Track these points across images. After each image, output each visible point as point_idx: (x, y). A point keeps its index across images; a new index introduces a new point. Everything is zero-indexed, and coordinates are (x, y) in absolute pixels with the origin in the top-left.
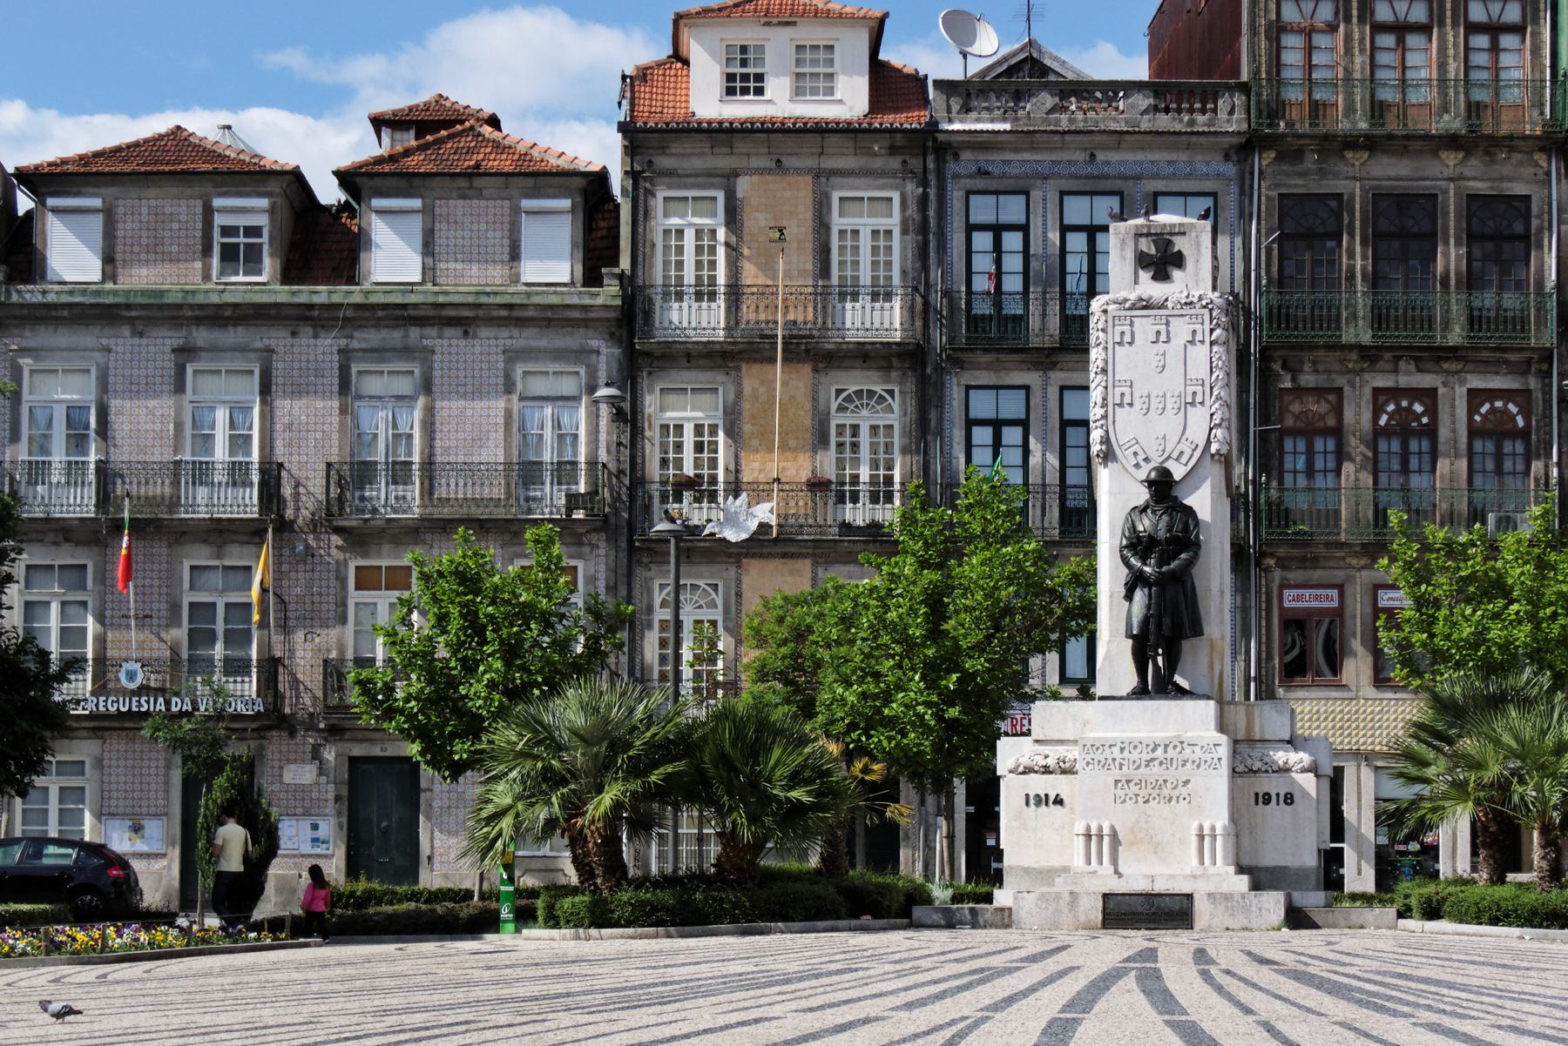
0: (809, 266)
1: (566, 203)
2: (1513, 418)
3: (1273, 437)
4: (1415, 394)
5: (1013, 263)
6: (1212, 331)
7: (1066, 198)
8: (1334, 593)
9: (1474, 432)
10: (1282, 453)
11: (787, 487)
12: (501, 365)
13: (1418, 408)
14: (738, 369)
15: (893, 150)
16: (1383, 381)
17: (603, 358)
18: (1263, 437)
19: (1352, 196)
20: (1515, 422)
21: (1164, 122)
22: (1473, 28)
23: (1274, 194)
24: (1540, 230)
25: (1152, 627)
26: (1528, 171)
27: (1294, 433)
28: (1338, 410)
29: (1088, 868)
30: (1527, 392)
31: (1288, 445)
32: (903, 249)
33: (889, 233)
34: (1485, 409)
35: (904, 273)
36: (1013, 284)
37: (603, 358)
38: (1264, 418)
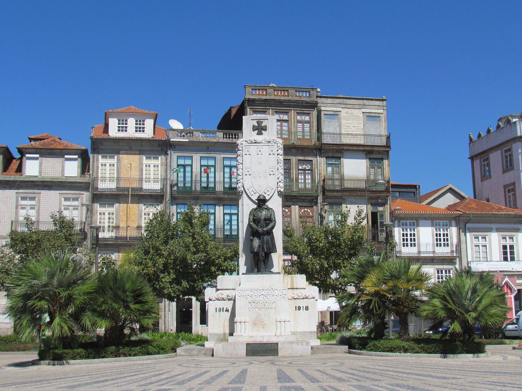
0: (138, 174)
1: (77, 157)
2: (309, 213)
5: (188, 174)
6: (278, 150)
8: (449, 195)
9: (300, 217)
11: (131, 228)
12: (58, 197)
13: (287, 210)
14: (119, 199)
15: (159, 146)
17: (85, 195)
21: (225, 140)
22: (299, 122)
24: (315, 168)
25: (261, 250)
32: (161, 170)
33: (158, 166)
34: (302, 211)
35: (161, 176)
36: (188, 179)
37: (85, 195)
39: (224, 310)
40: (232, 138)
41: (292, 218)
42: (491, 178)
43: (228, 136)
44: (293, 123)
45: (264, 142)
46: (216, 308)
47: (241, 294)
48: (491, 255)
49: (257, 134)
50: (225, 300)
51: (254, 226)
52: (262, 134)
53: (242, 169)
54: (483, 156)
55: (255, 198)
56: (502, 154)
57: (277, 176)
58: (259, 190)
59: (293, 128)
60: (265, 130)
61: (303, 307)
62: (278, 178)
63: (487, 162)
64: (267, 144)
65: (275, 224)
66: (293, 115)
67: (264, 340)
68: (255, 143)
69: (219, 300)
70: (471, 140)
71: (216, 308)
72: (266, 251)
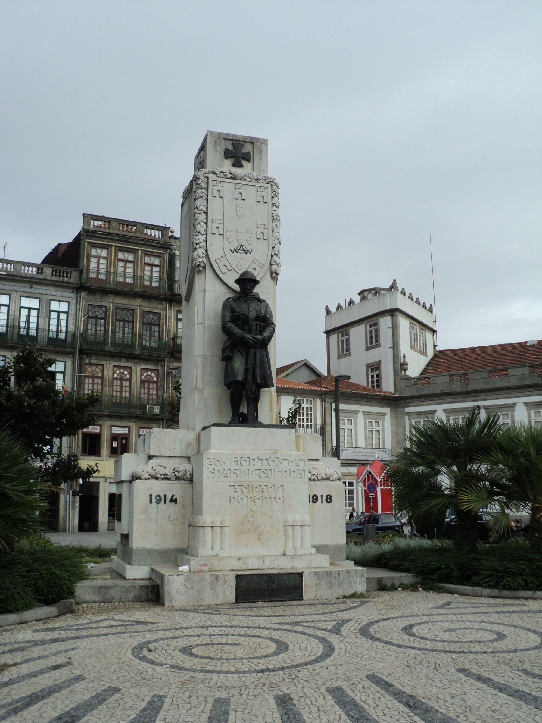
2: (153, 378)
3: (82, 378)
4: (125, 368)
6: (273, 197)
7: (22, 298)
9: (142, 382)
10: (85, 383)
13: (126, 373)
16: (115, 364)
18: (79, 378)
19: (110, 307)
20: (154, 379)
21: (54, 278)
23: (87, 304)
24: (163, 323)
26: (160, 306)
27: (89, 377)
28: (103, 371)
29: (214, 553)
30: (158, 370)
31: (87, 380)
38: (80, 372)
39: (168, 501)
40: (63, 276)
41: (132, 382)
42: (350, 355)
43: (58, 274)
44: (139, 265)
45: (248, 179)
46: (151, 496)
47: (214, 467)
48: (356, 441)
49: (234, 165)
50: (168, 479)
51: (237, 331)
52: (241, 166)
53: (206, 223)
54: (341, 330)
55: (231, 279)
56: (338, 338)
57: (270, 244)
58: (237, 266)
59: (139, 272)
60: (249, 161)
61: (322, 496)
62: (273, 248)
63: (347, 337)
64: (254, 184)
65: (274, 331)
66: (140, 257)
67: (266, 565)
68: (231, 178)
69: (157, 479)
70: (328, 312)
71: (151, 496)
72: (259, 381)
